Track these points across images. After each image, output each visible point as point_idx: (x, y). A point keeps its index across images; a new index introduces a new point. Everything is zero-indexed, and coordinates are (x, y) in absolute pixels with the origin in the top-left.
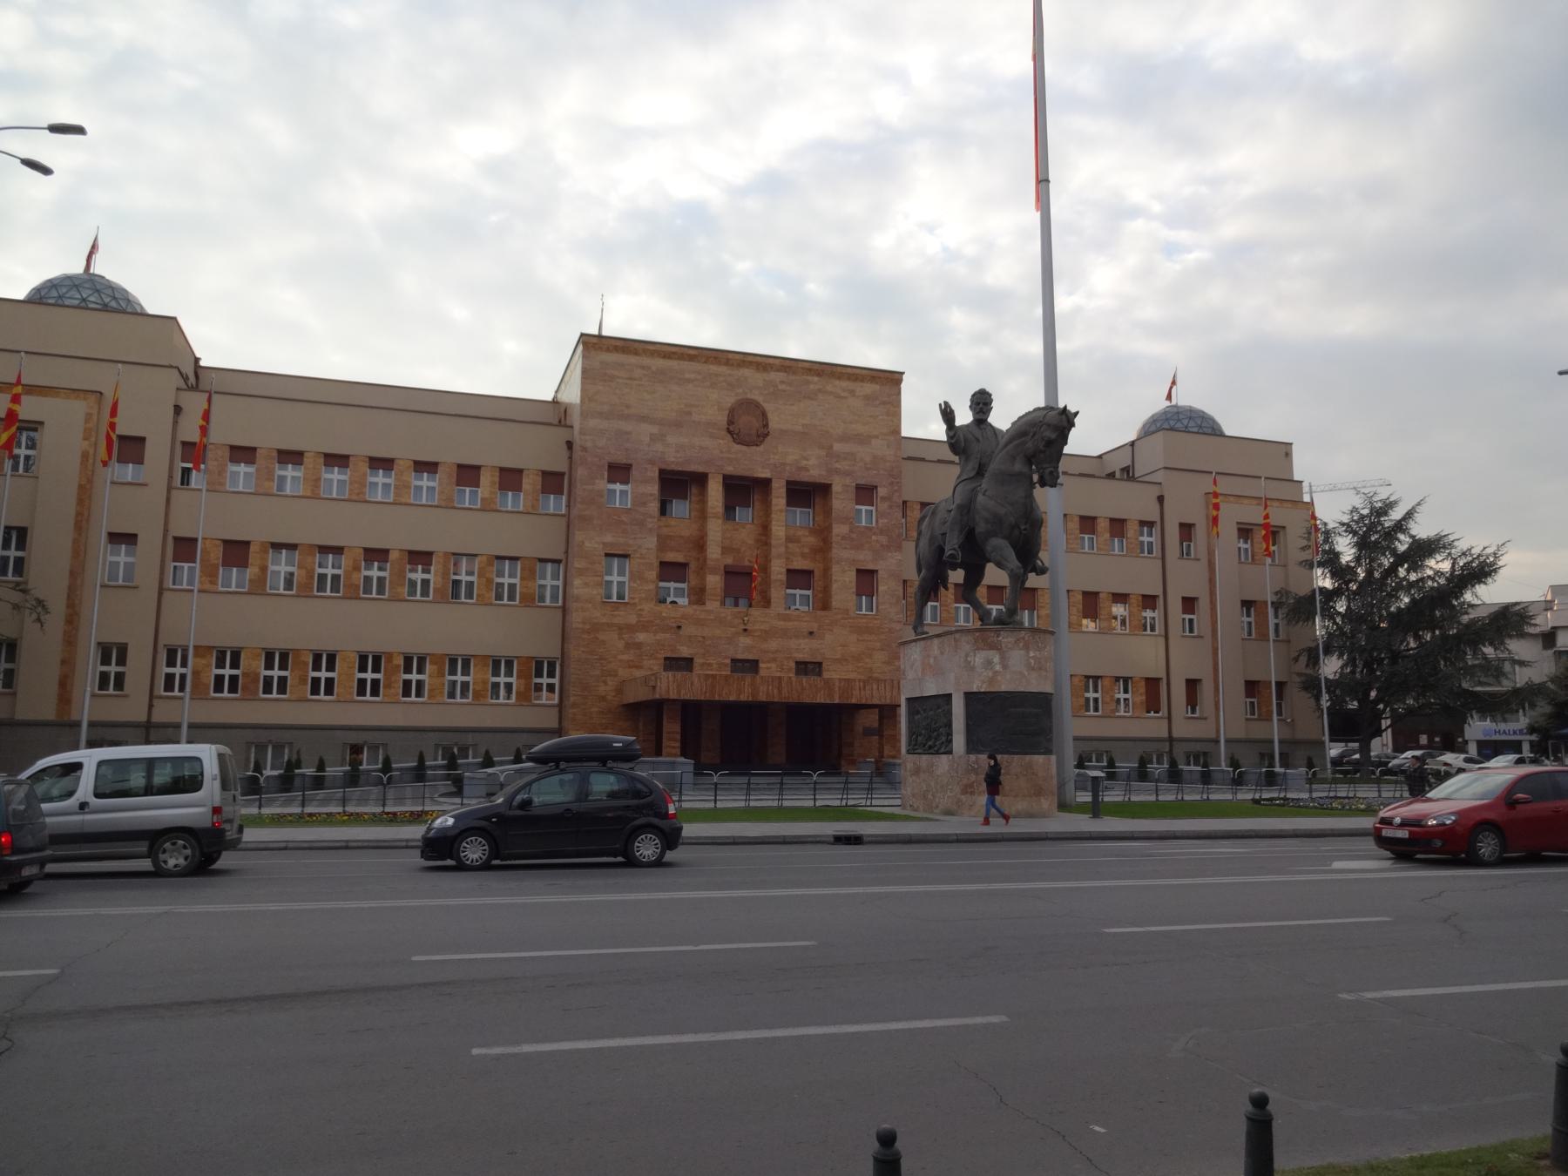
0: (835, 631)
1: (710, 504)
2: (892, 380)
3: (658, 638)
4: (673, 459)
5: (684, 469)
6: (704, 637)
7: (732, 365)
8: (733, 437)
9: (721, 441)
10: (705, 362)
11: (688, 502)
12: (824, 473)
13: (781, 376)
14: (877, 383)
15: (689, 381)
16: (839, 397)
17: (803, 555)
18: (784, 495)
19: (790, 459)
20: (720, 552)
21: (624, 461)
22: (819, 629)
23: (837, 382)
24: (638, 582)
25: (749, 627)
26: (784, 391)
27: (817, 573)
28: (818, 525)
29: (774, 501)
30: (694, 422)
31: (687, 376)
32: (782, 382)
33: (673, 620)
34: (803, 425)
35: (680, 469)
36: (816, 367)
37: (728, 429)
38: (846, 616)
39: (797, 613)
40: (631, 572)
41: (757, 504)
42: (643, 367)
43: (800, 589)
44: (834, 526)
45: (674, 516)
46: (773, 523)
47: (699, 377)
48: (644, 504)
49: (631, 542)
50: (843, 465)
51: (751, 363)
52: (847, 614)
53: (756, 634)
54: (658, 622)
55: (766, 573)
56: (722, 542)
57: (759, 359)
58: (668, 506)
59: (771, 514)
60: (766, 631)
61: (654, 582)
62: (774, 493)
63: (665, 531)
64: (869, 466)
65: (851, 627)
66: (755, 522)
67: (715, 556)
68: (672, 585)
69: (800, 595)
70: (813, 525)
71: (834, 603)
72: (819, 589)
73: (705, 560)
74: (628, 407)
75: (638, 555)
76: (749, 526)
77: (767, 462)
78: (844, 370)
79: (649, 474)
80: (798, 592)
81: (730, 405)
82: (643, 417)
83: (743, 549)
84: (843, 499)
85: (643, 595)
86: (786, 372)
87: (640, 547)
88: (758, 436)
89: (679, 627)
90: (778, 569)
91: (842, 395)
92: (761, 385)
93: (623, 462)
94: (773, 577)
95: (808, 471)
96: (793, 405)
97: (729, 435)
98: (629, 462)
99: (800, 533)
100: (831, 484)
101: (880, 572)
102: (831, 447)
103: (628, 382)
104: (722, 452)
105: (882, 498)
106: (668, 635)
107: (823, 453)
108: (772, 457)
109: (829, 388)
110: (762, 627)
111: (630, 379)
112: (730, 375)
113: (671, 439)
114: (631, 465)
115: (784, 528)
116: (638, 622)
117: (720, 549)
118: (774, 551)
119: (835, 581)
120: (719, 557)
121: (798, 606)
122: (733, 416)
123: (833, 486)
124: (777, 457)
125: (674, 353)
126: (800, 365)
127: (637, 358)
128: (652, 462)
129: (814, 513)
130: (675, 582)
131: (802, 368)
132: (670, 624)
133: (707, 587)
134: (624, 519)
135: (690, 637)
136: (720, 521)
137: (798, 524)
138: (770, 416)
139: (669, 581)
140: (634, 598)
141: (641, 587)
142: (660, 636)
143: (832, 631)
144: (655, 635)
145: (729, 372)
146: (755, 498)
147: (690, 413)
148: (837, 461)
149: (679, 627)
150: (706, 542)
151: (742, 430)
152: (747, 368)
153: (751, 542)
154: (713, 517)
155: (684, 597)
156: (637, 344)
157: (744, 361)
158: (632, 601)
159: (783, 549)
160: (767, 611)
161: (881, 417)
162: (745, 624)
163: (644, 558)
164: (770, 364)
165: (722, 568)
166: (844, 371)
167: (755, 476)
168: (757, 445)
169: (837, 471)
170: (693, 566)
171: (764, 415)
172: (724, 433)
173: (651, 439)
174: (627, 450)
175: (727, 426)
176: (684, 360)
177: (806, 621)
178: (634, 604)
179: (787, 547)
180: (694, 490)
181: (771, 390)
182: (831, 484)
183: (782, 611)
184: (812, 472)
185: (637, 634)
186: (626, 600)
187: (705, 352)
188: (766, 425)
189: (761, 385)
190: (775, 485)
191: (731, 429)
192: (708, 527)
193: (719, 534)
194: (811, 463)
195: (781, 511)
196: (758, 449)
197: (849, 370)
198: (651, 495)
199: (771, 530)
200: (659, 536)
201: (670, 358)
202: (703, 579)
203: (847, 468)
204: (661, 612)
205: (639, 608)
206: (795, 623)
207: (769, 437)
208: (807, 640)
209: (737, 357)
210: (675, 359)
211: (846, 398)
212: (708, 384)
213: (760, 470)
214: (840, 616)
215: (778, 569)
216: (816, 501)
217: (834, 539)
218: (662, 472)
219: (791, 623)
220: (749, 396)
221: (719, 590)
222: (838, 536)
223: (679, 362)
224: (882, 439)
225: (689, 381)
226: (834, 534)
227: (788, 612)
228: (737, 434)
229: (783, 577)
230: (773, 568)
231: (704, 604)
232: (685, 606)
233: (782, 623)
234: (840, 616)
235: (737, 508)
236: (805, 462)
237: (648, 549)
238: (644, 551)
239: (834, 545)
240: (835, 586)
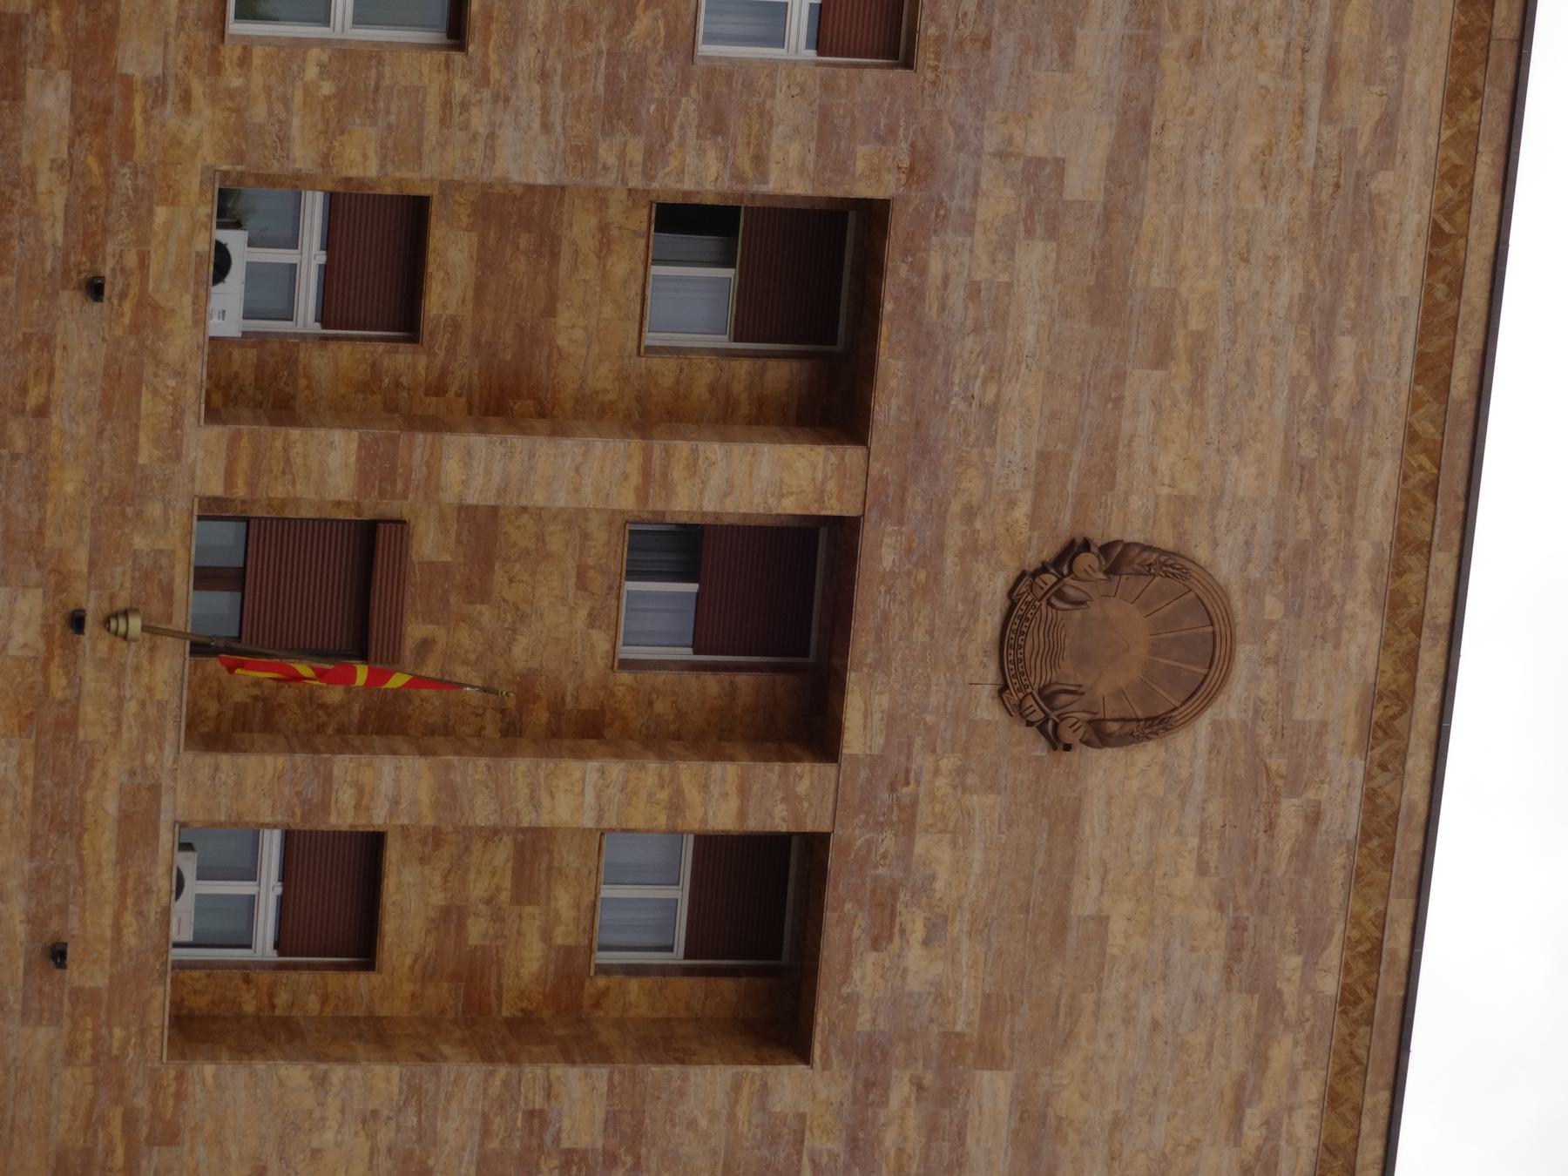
0: (67, 1075)
1: (714, 451)
3: (45, 180)
4: (936, 268)
5: (884, 330)
6: (42, 412)
7: (1399, 571)
8: (1044, 569)
9: (1021, 512)
10: (1412, 436)
11: (723, 341)
12: (864, 1021)
13: (1345, 817)
15: (1321, 357)
16: (1239, 1107)
17: (451, 917)
18: (753, 825)
19: (933, 849)
20: (472, 499)
21: (928, 30)
22: (77, 994)
23: (1312, 1088)
24: (327, 88)
25: (93, 641)
26: (1270, 828)
27: (361, 983)
28: (604, 993)
29: (726, 773)
30: (1120, 377)
31: (1346, 346)
32: (1314, 818)
33: (131, 259)
34: (1102, 920)
35: (888, 307)
36: (1389, 987)
37: (1086, 545)
38: (144, 1131)
39: (164, 884)
40: (376, 53)
41: (712, 684)
42: (1387, 126)
43: (283, 901)
44: (601, 1073)
45: (656, 270)
46: (616, 769)
47: (1340, 403)
48: (715, 125)
49: (527, 54)
51: (1410, 660)
52: (151, 1141)
53: (58, 682)
54: (125, 182)
55: (361, 730)
56: (525, 509)
57: (1426, 702)
58: (705, 244)
59: (663, 755)
60: (69, 724)
61: (325, 161)
62: (769, 773)
63: (580, 228)
65: (88, 1154)
66: (625, 677)
67: (452, 470)
68: (310, 257)
69: (251, 900)
70: (605, 970)
71: (209, 1069)
72: (282, 998)
73: (434, 425)
74: (1194, 53)
75: (461, 87)
76: (603, 645)
77: (918, 741)
78: (1371, 1127)
79: (864, 152)
80: (268, 889)
81: (1202, 553)
82: (1145, 126)
83: (485, 613)
84: (732, 1118)
85: (258, 113)
86: (1366, 835)
87: (501, 99)
88: (1047, 696)
89: (95, 289)
90: (386, 785)
91: (1253, 1117)
92: (1298, 714)
93: (922, 19)
94: (343, 765)
95: (876, 945)
96: (1202, 869)
97: (1048, 554)
98: (925, 55)
99: (563, 900)
100: (805, 1057)
102: (990, 1057)
103: (1317, 58)
104: (970, 513)
106: (54, 233)
107: (964, 1019)
108: (949, 763)
109: (1284, 1051)
110: (88, 711)
111: (1332, 66)
112: (1350, 557)
113: (1034, 258)
114: (908, 64)
115: (588, 821)
116: (127, 81)
117: (492, 502)
118: (473, 770)
119: (322, 1082)
120: (450, 497)
121: (193, 887)
122: (1148, 570)
123: (801, 1068)
124: (942, 783)
126: (1400, 908)
127: (1437, 98)
128: (921, 167)
129: (664, 971)
130: (326, 272)
131: (1381, 921)
132: (110, 247)
133: (295, 433)
134: (642, 24)
135: (47, 342)
136: (626, 501)
137: (607, 892)
138: (1146, 754)
139: (328, 244)
140: (244, 61)
141: (298, 97)
142: (53, 196)
143: (71, 1053)
144: (57, 167)
145: (1365, 551)
146: (742, 679)
147: (1162, 357)
148: (919, 1086)
149: (95, 289)
150: (523, 431)
151: (1078, 614)
152: (1385, 645)
153: (521, 656)
154: (646, 472)
155: (248, 315)
156: (1504, 100)
157: (1416, 626)
158: (230, 53)
159: (483, 812)
160: (173, 734)
162: (107, 622)
163: (444, 122)
164: (1402, 755)
165: (393, 508)
166: (1366, 1125)
167: (852, 677)
168: (1003, 689)
169: (871, 1089)
170: (404, 361)
171: (1156, 725)
172: (1065, 527)
173: (1040, 162)
174: (986, 43)
175: (1098, 540)
176: (1424, 334)
177: (117, 928)
178: (216, 68)
179: (493, 834)
180: (781, 374)
181: (1277, 763)
182: (805, 1057)
183: (175, 805)
184: (871, 957)
185: (64, 80)
186: (236, 28)
187: (1464, 436)
188: (1099, 735)
189: (1298, 714)
190: (808, 776)
191: (1086, 561)
192: (599, 445)
193: (562, 500)
194: (915, 956)
195: (676, 805)
196: (986, 693)
198: (760, 160)
199: (578, 755)
200: (553, 195)
201: (1432, 263)
202: (341, 412)
203: (890, 1138)
204: (173, 202)
205: (197, 88)
206: (109, 875)
207: (1040, 749)
208: (21, 930)
209: (1439, 595)
210: (1429, 290)
211: (1237, 1123)
212: (1308, 451)
213: (883, 701)
214: (141, 1101)
215: (386, 785)
216: (726, 985)
217: (533, 1073)
218: (874, 214)
219: (109, 855)
220: (1245, 653)
221: (279, 491)
222: (548, 1094)
223: (1414, 302)
225: (1321, 357)
226: (558, 1070)
227: (166, 839)
228: (1060, 595)
229: (343, 817)
230: (387, 764)
231: (213, 415)
232: (200, 316)
233: (112, 807)
234: (141, 1101)
235: (693, 587)
236: (917, 932)
237: (492, 136)
238: (479, 120)
239: (503, 1071)
240: (296, 1074)
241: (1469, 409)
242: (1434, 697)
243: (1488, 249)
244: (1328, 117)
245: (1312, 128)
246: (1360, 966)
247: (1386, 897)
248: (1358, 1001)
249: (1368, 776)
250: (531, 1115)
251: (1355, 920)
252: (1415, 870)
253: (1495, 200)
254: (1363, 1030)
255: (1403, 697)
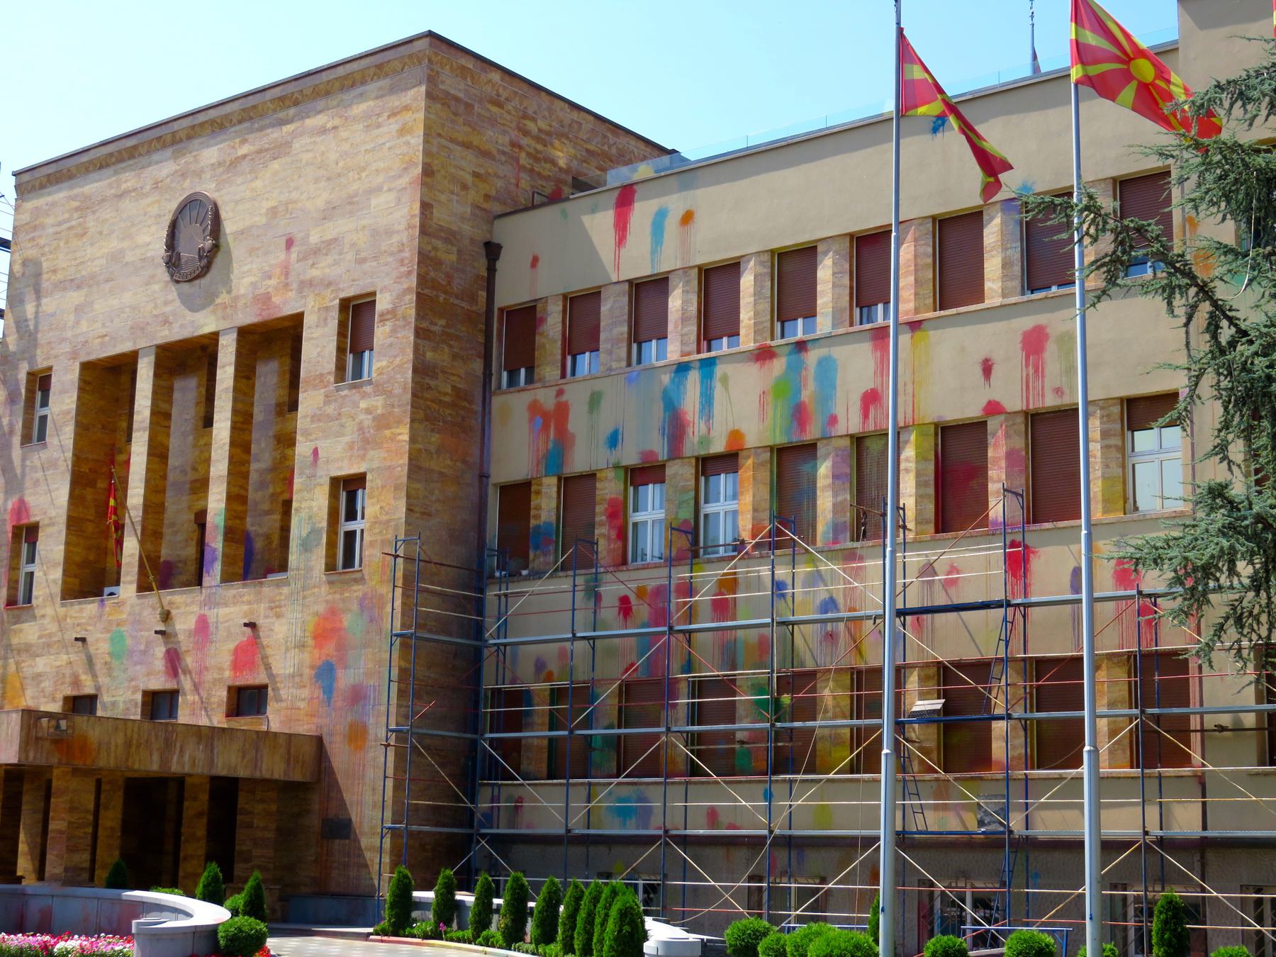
2: (410, 56)
14: (387, 75)
50: (322, 269)
51: (202, 125)
57: (213, 114)
64: (363, 255)
101: (369, 477)
105: (382, 315)
116: (40, 637)
125: (111, 155)
126: (269, 95)
131: (272, 101)
138: (223, 214)
157: (193, 127)
161: (388, 145)
164: (226, 116)
167: (196, 334)
197: (341, 71)
210: (114, 164)
224: (390, 190)
241: (139, 136)
242: (211, 111)
243: (102, 148)
244: (69, 220)
245: (74, 223)
246: (287, 103)
247: (265, 103)
248: (297, 98)
249: (235, 125)
250: (312, 421)
251: (275, 111)
252: (259, 95)
253: (92, 151)
254: (304, 92)
255: (212, 122)
